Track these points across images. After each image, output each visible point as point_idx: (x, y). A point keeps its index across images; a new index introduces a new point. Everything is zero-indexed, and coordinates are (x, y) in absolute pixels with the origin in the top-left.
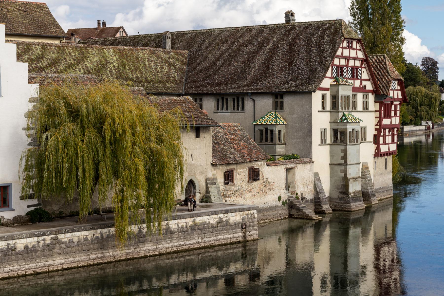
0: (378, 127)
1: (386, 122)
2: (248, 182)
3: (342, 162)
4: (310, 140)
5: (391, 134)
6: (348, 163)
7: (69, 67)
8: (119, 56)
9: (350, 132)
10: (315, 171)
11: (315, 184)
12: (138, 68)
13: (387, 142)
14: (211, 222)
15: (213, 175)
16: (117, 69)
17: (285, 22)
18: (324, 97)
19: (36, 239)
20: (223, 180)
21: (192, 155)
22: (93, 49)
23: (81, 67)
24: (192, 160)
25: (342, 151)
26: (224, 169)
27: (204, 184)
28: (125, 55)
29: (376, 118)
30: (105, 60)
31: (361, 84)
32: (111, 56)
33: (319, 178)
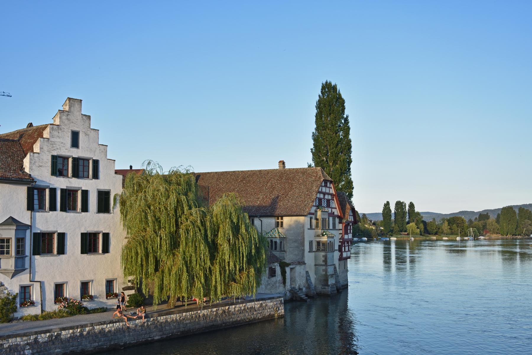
0: (342, 240)
1: (346, 237)
3: (324, 263)
4: (303, 248)
5: (348, 245)
9: (328, 243)
13: (346, 251)
18: (311, 218)
25: (323, 256)
29: (340, 234)
33: (309, 275)
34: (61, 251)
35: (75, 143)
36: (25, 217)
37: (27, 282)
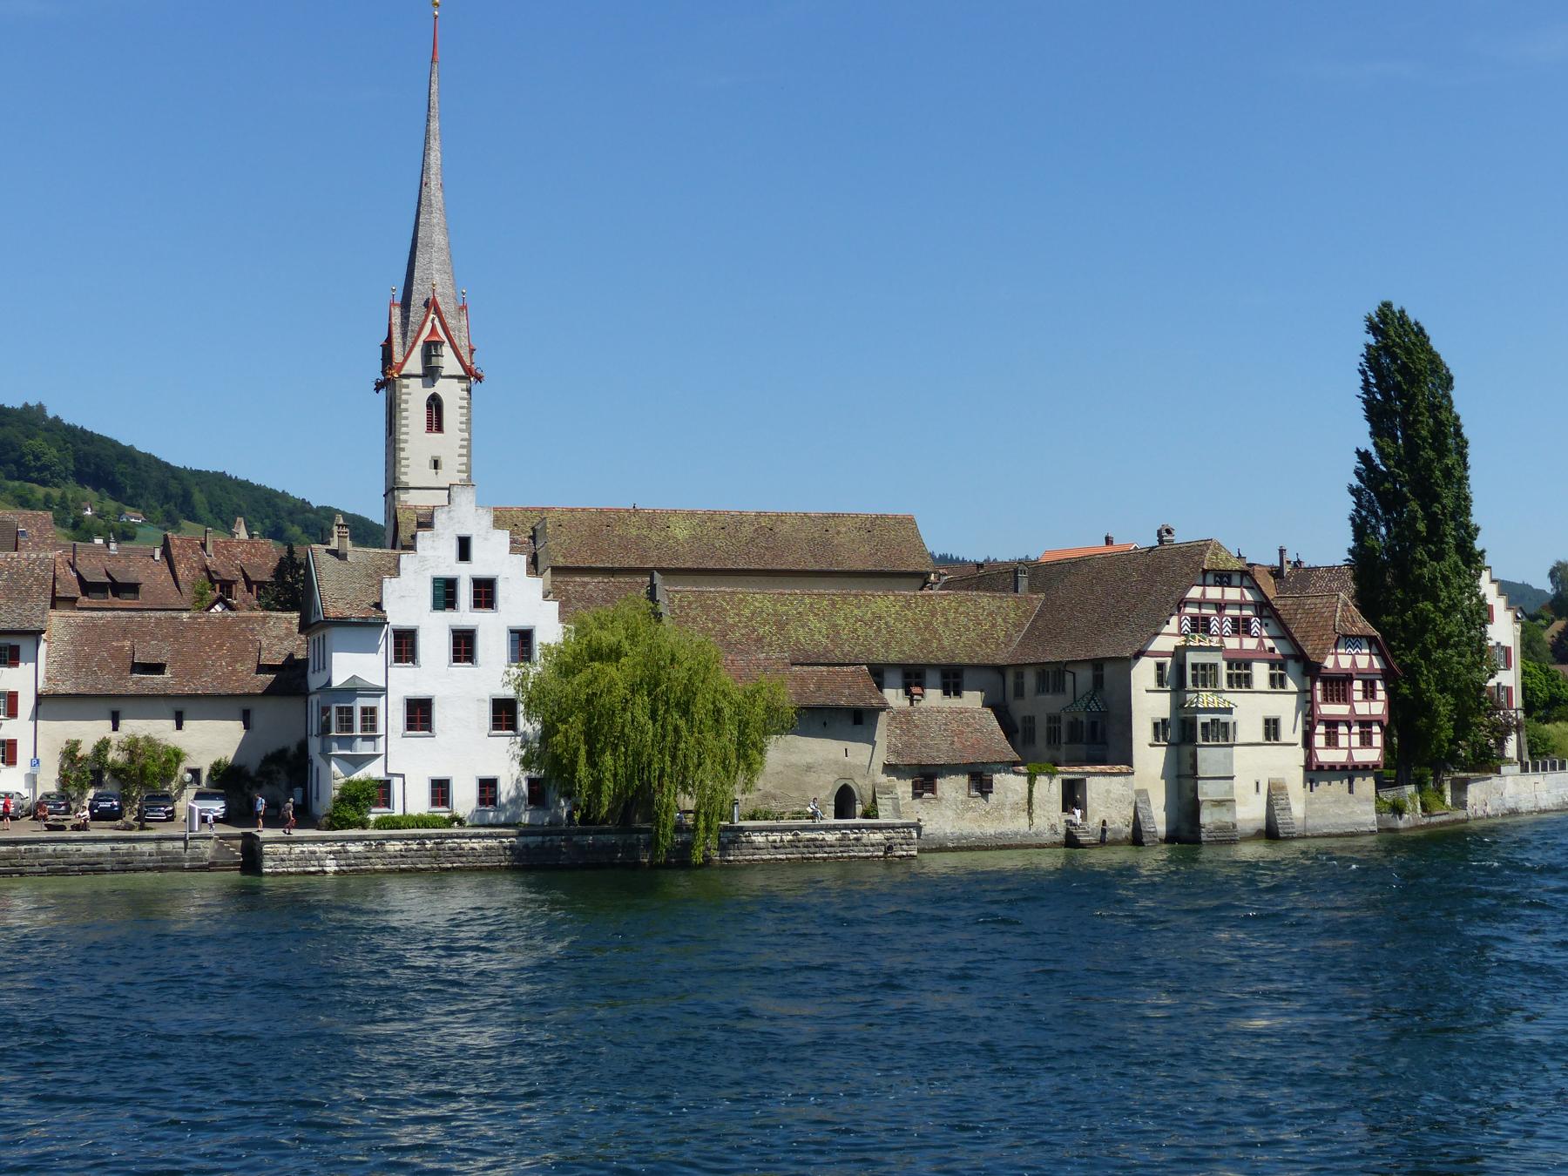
0: (1310, 719)
2: (969, 795)
6: (1201, 774)
7: (802, 626)
10: (1137, 787)
11: (1136, 808)
12: (932, 624)
16: (889, 627)
18: (1160, 666)
19: (540, 839)
22: (856, 596)
23: (824, 625)
27: (870, 793)
28: (913, 605)
30: (873, 613)
31: (1261, 643)
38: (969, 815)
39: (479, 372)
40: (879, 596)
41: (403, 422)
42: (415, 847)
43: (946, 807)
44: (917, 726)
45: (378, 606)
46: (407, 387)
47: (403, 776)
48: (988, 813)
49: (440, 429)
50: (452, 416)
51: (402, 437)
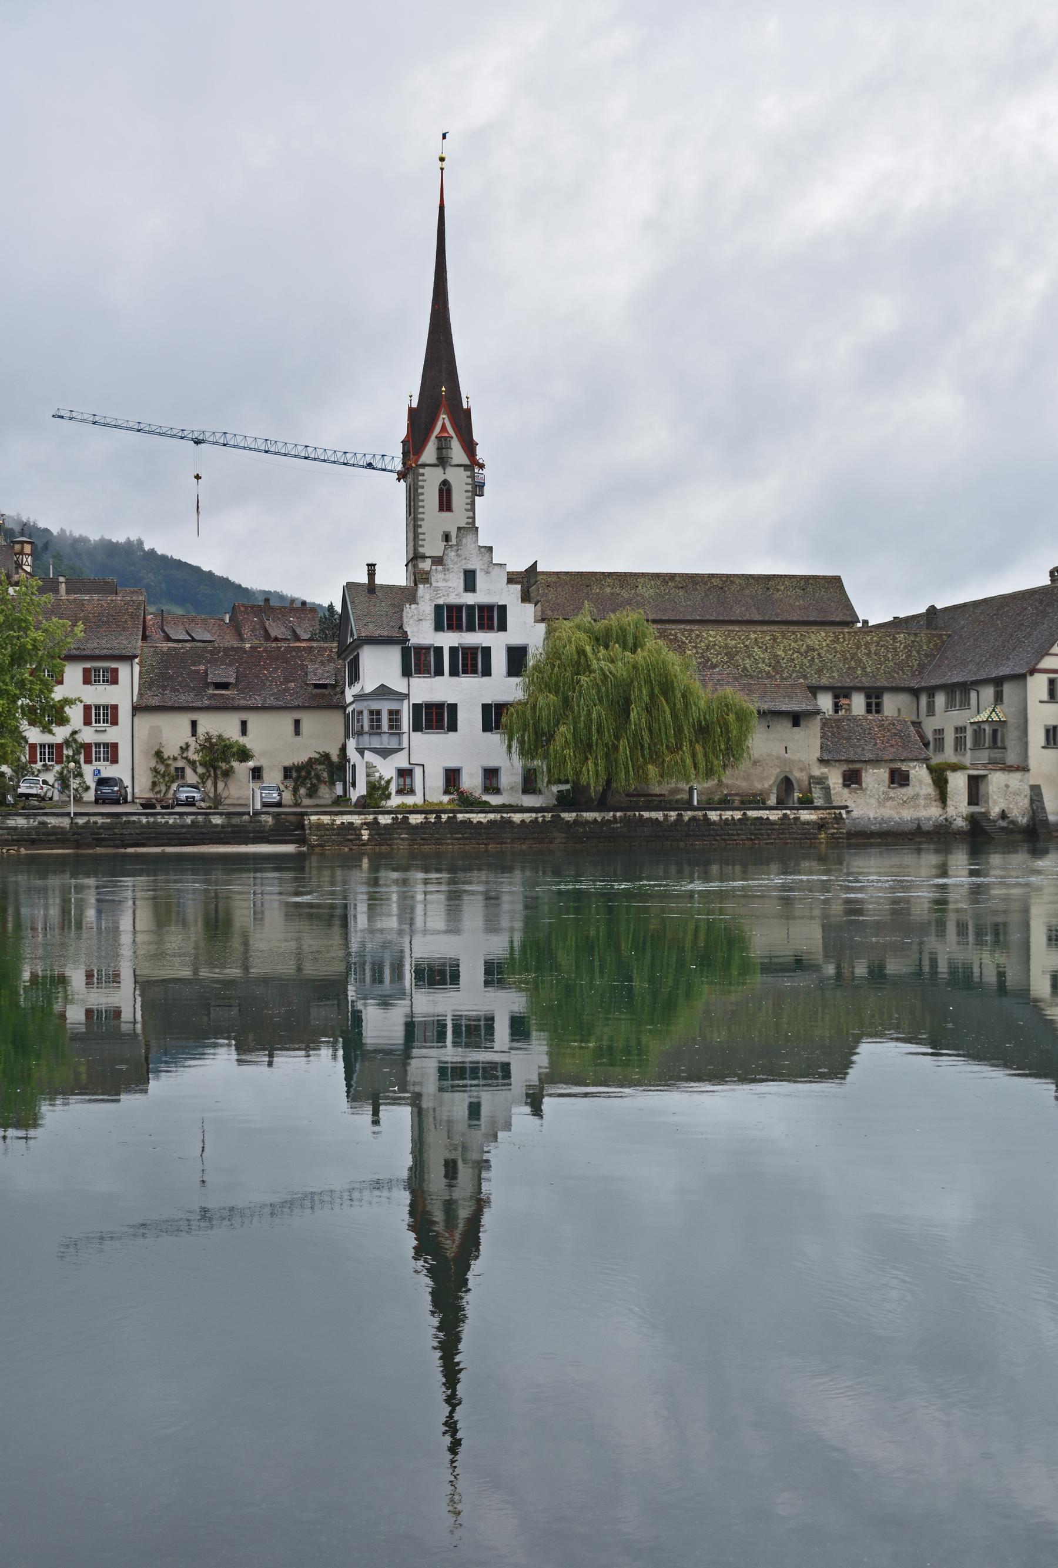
7: (749, 657)
8: (831, 641)
10: (1032, 782)
12: (857, 655)
14: (771, 818)
15: (822, 773)
16: (821, 657)
17: (1049, 583)
19: (534, 815)
20: (840, 781)
21: (786, 748)
22: (794, 633)
24: (786, 753)
26: (845, 767)
27: (807, 783)
28: (841, 640)
30: (808, 646)
32: (819, 641)
34: (453, 727)
35: (470, 585)
36: (399, 685)
37: (405, 765)
38: (889, 803)
39: (481, 461)
40: (813, 632)
41: (420, 504)
42: (433, 821)
43: (870, 796)
44: (845, 730)
45: (401, 627)
46: (423, 475)
47: (423, 765)
48: (905, 802)
49: (449, 509)
50: (459, 498)
51: (420, 516)
